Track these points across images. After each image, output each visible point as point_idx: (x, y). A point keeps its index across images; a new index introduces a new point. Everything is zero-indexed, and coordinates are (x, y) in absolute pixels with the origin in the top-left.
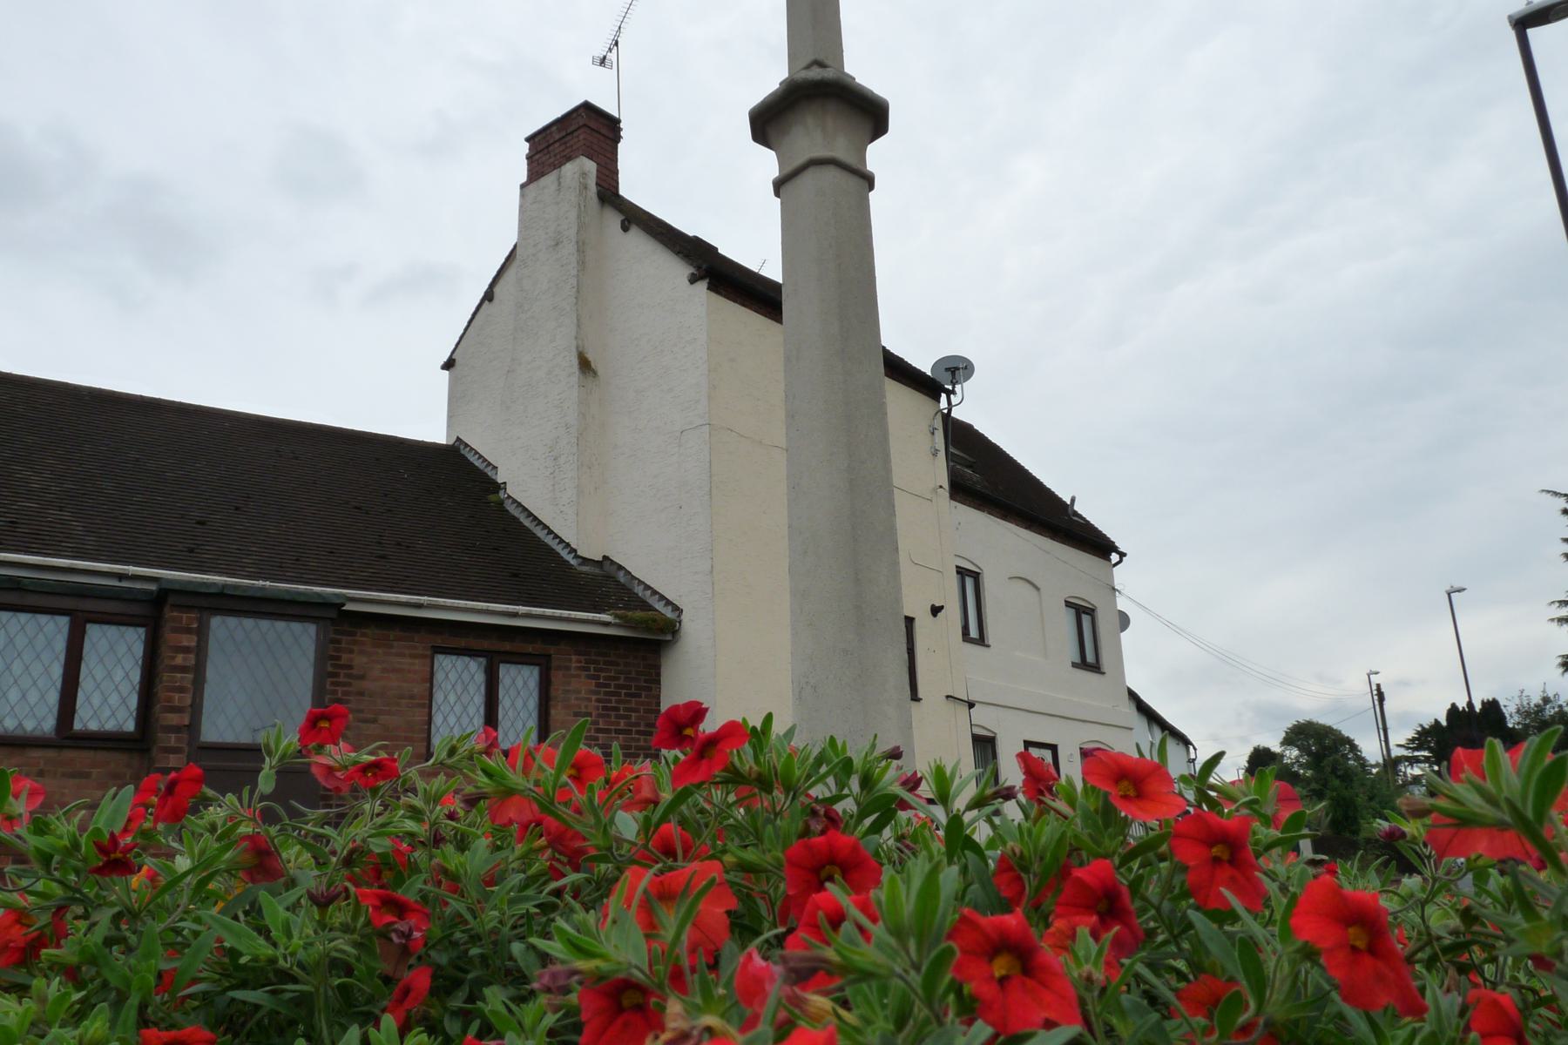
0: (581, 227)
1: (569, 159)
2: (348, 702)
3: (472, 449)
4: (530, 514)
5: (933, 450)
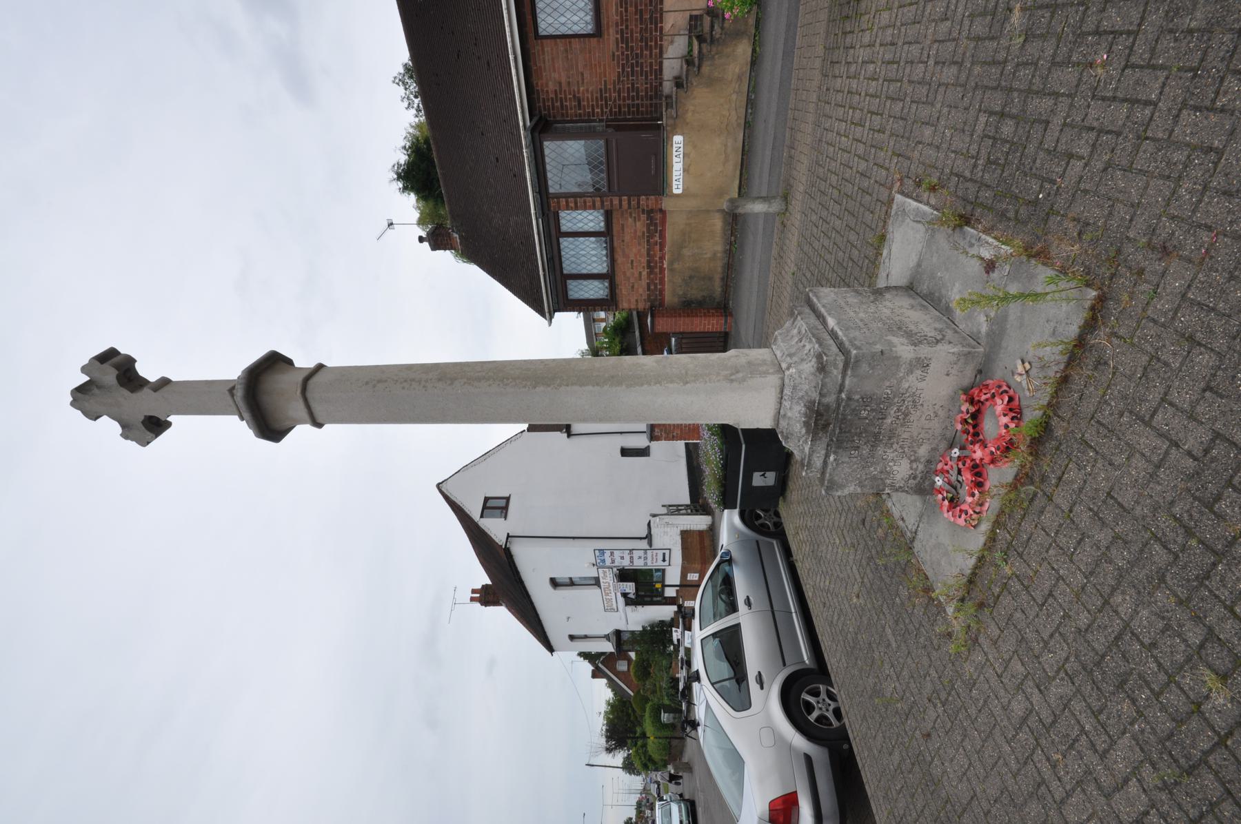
2: (574, 91)
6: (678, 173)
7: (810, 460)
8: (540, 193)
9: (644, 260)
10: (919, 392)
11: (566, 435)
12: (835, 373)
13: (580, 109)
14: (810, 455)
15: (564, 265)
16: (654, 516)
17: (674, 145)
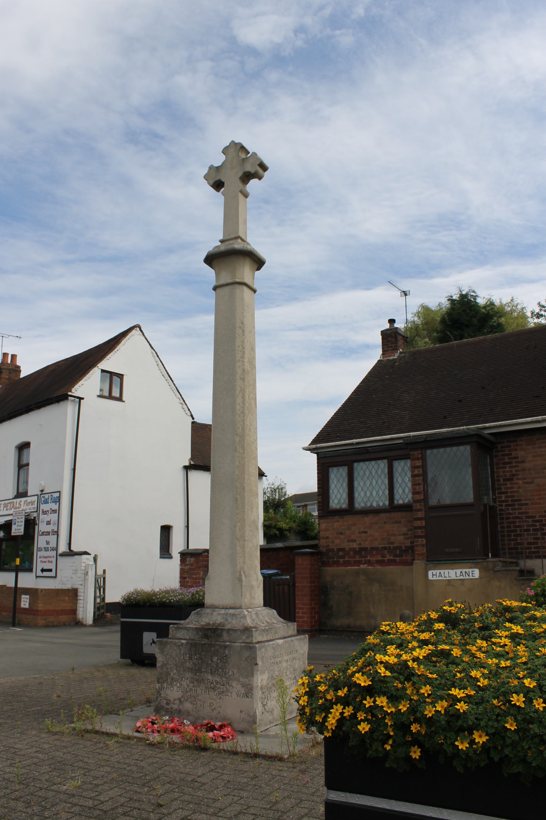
2: (518, 475)
6: (446, 575)
7: (182, 628)
8: (426, 441)
9: (367, 544)
10: (229, 694)
11: (187, 464)
13: (504, 480)
15: (361, 464)
16: (95, 559)
17: (470, 570)
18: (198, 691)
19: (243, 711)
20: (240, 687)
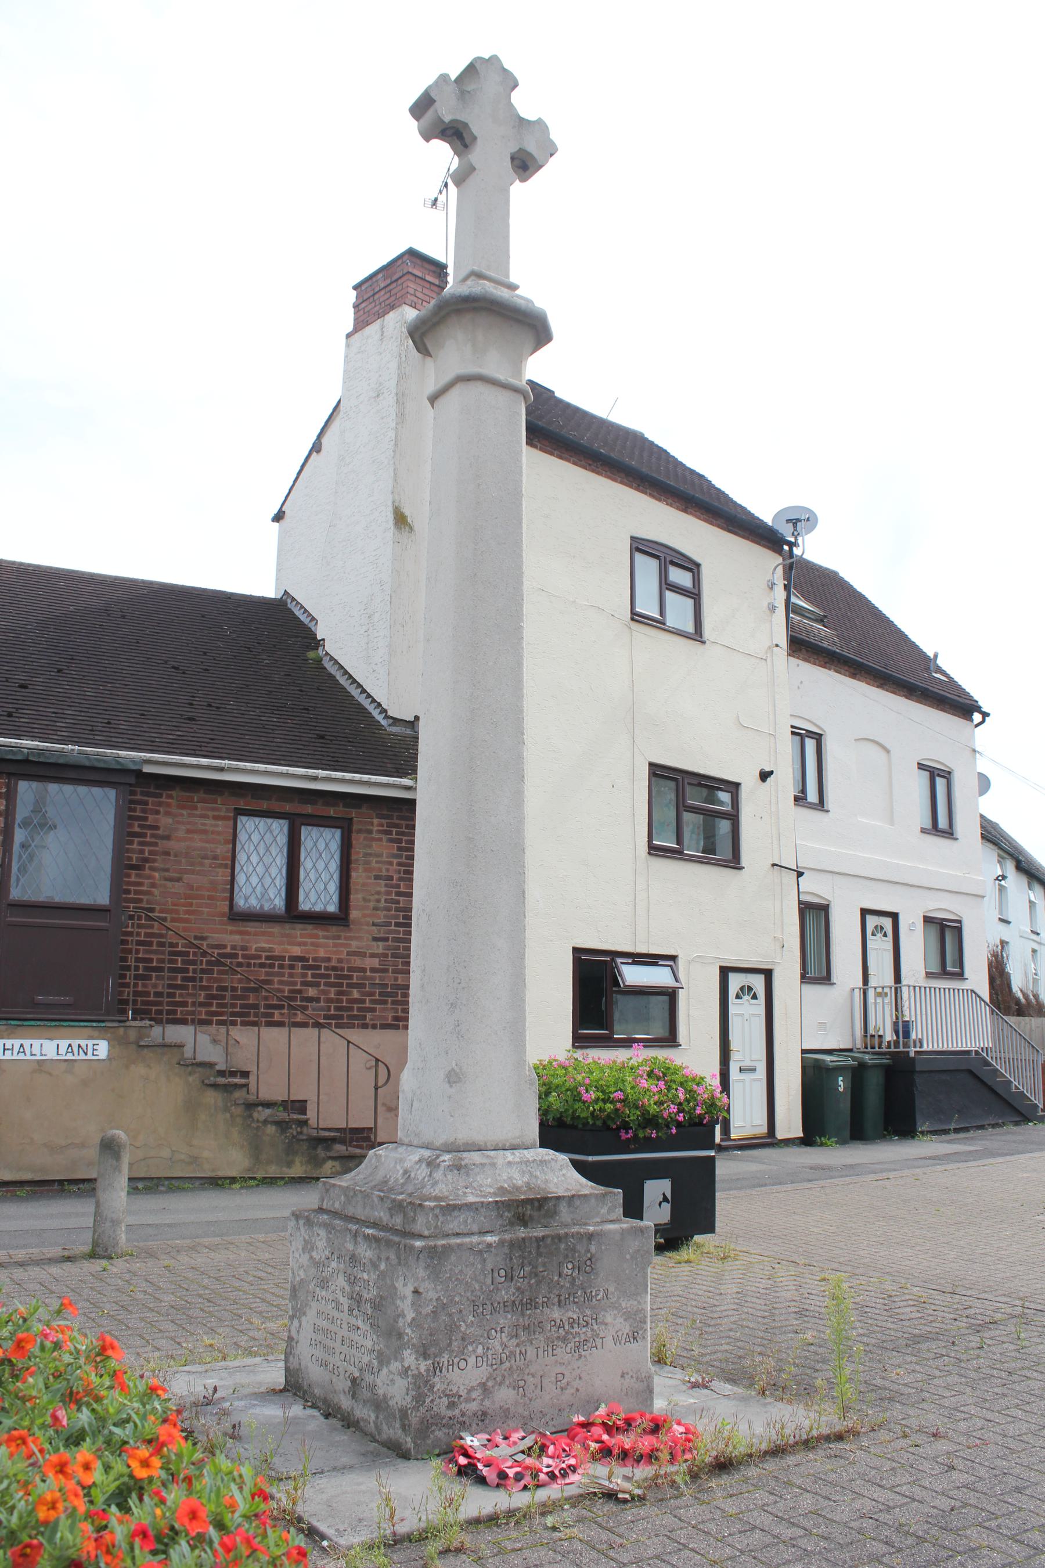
0: (401, 377)
1: (392, 307)
2: (154, 861)
3: (298, 603)
4: (346, 672)
5: (771, 606)
6: (36, 1050)
8: (26, 761)
12: (602, 1211)
14: (469, 1206)
17: (90, 1043)
18: (529, 1353)
19: (628, 1374)
20: (621, 1320)
